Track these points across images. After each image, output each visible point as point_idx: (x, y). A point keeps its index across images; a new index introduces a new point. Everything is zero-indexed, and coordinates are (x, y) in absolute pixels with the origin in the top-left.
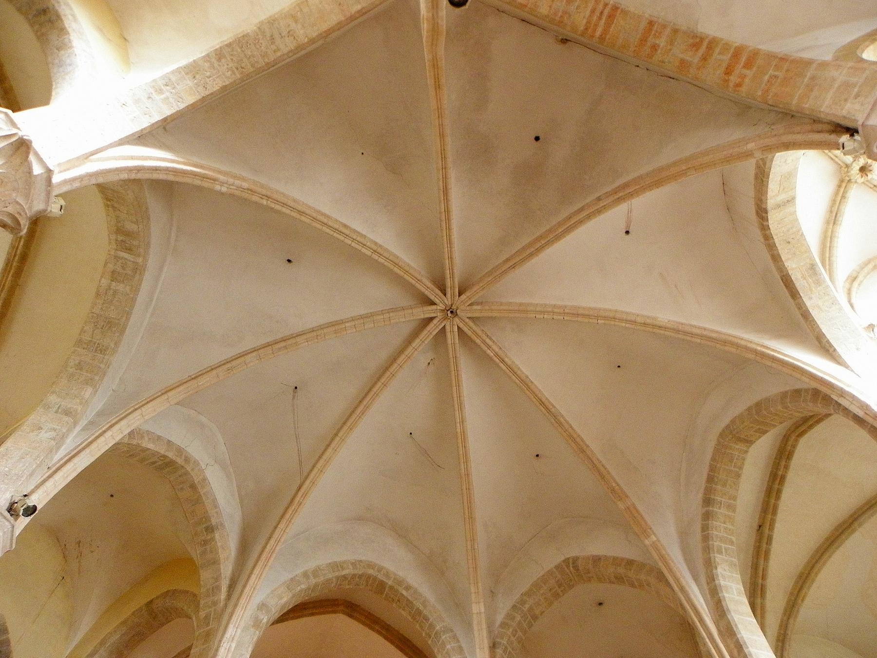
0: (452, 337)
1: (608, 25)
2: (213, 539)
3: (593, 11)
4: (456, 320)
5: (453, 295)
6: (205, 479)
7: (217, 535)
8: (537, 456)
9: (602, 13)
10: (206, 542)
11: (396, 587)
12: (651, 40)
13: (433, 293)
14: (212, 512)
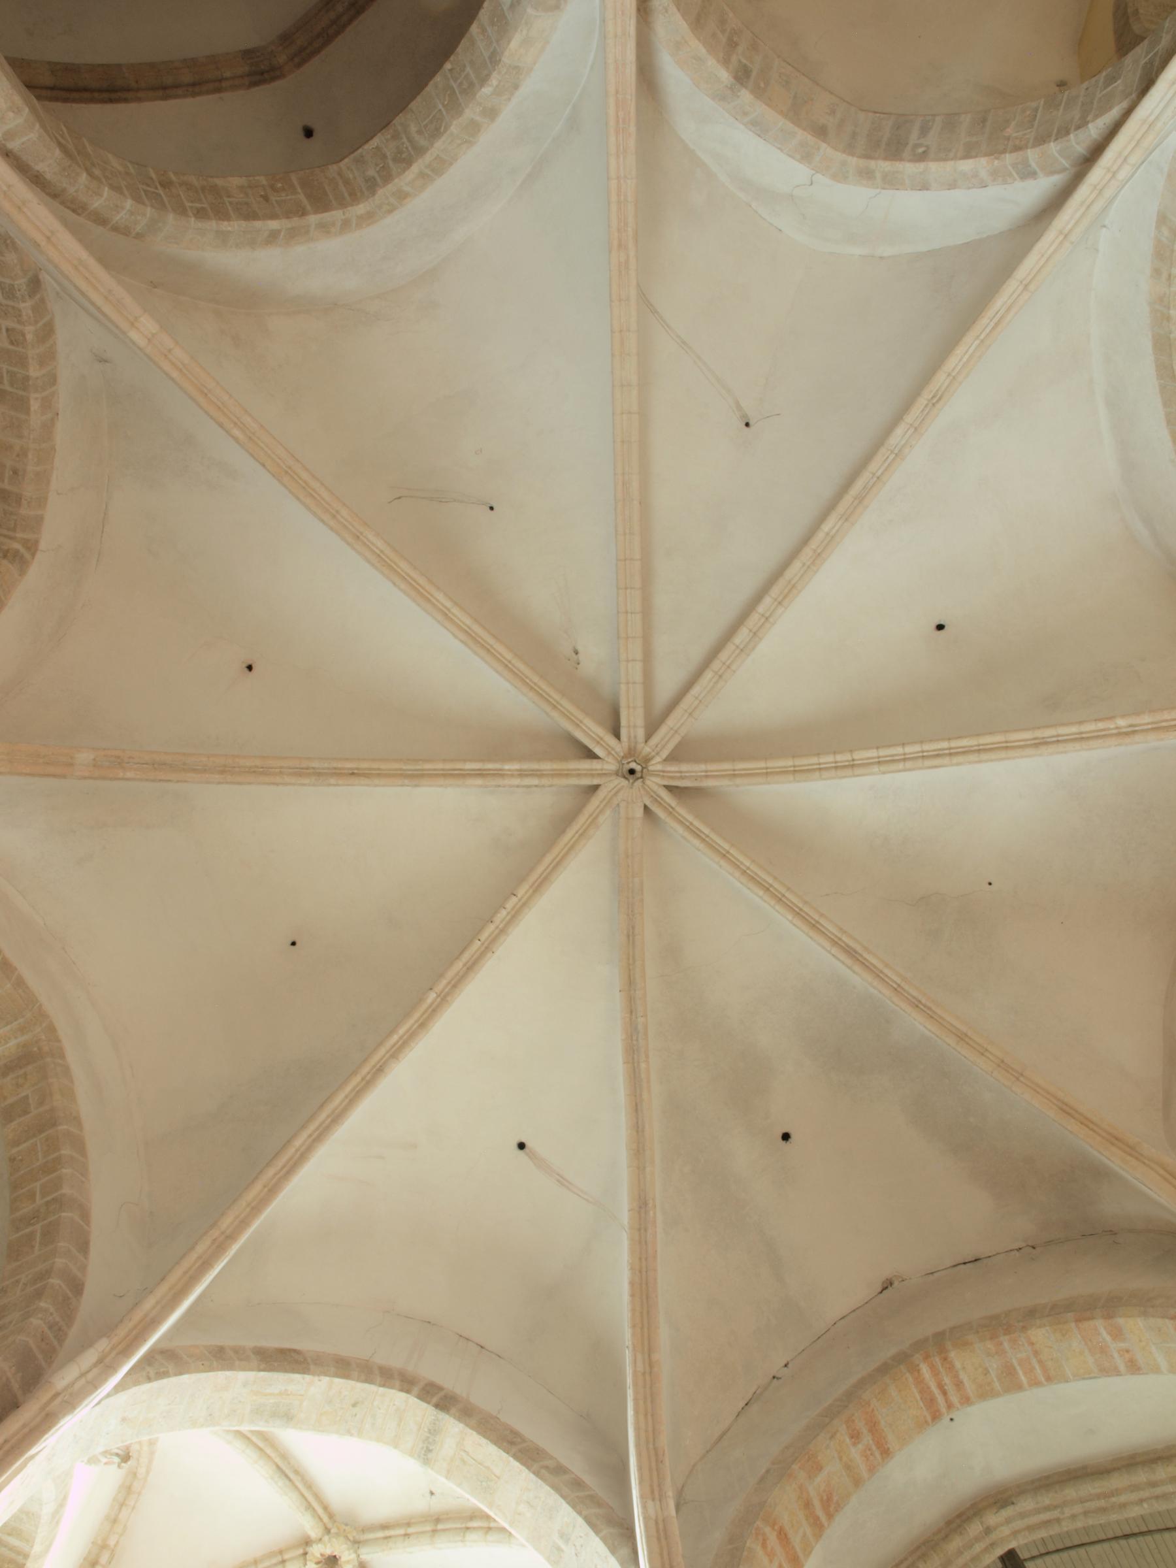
0: (592, 732)
1: (924, 1390)
2: (726, 62)
3: (959, 1385)
4: (611, 765)
5: (657, 800)
6: (806, 157)
7: (725, 76)
8: (250, 668)
9: (945, 1393)
10: (732, 45)
11: (296, 221)
12: (867, 1439)
13: (689, 772)
14: (760, 109)
